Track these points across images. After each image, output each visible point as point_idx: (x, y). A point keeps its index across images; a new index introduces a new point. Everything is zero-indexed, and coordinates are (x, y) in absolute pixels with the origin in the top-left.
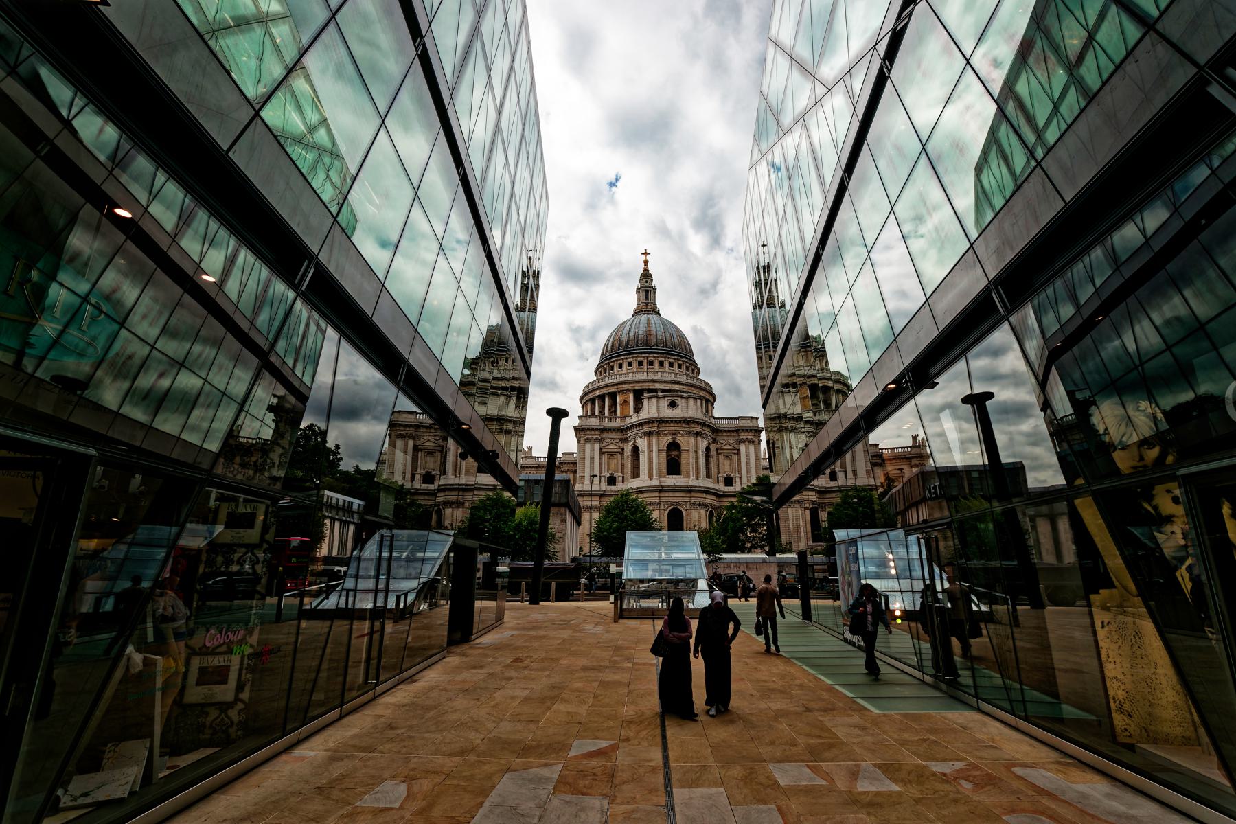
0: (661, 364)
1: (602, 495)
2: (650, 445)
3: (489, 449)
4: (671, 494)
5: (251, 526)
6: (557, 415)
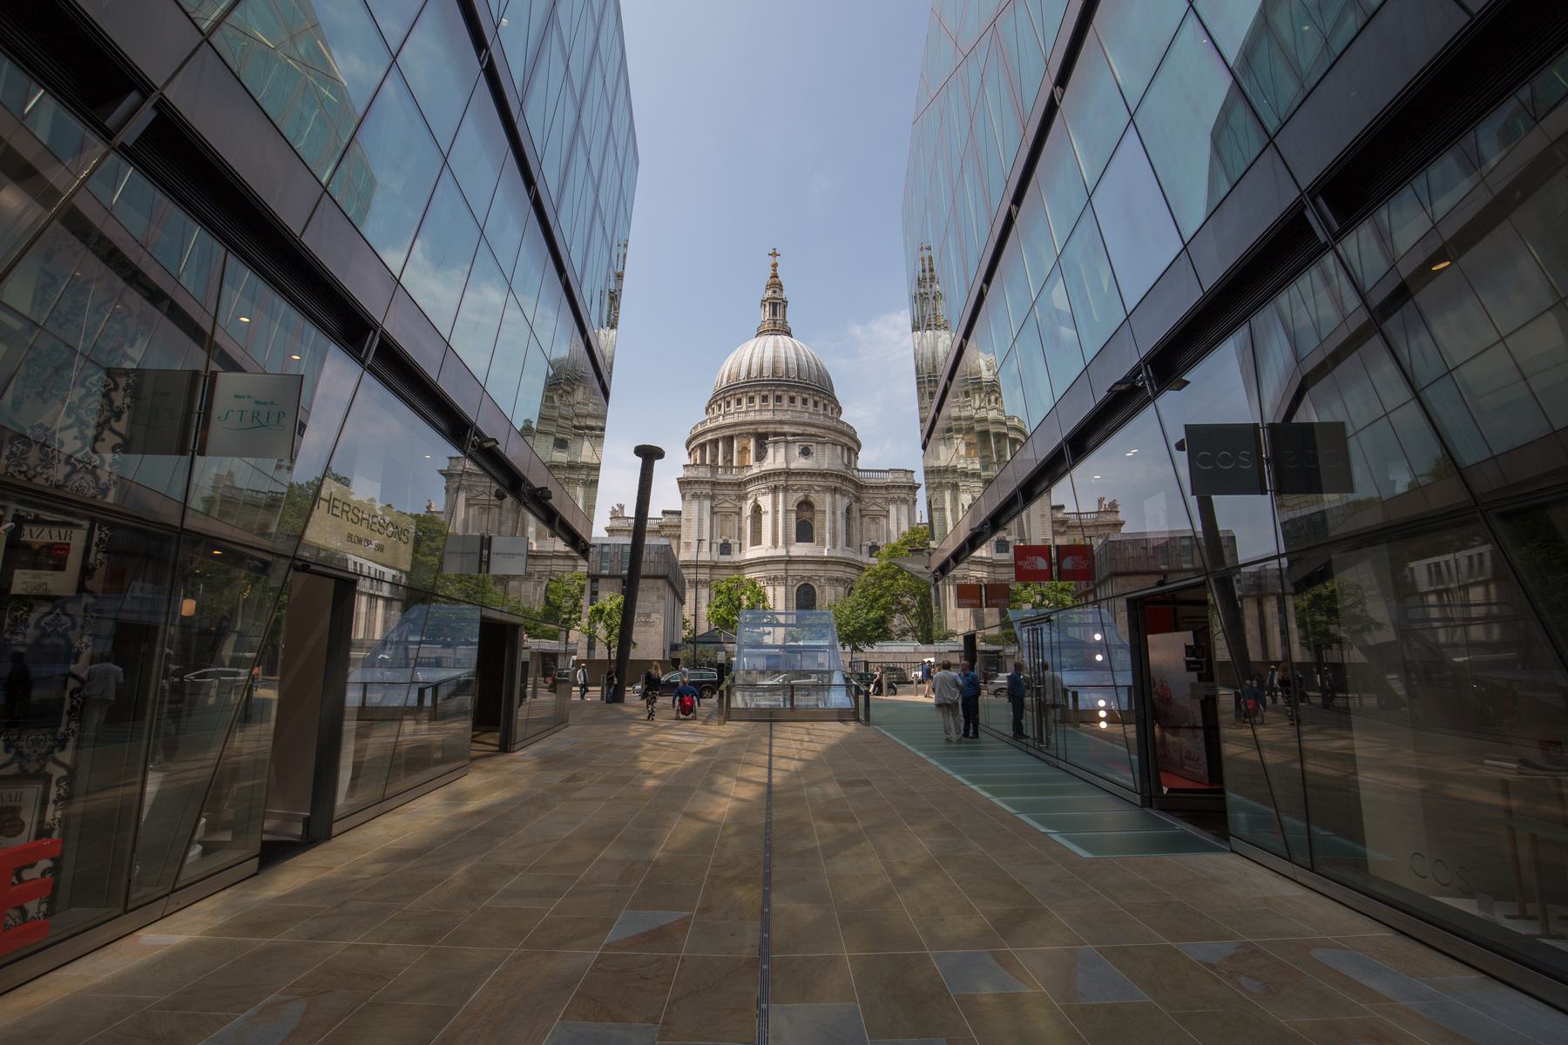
0: (792, 400)
1: (714, 567)
2: (775, 504)
3: (537, 485)
4: (801, 566)
5: (60, 566)
6: (649, 455)
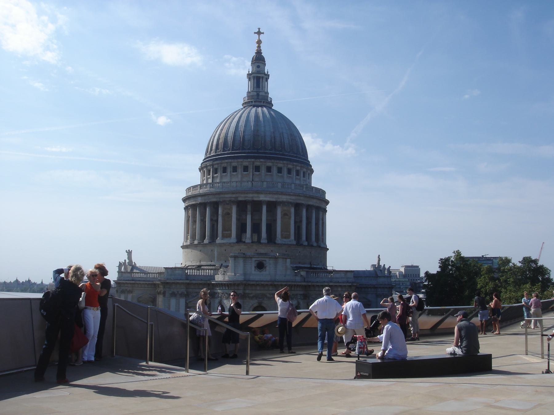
0: (269, 169)
